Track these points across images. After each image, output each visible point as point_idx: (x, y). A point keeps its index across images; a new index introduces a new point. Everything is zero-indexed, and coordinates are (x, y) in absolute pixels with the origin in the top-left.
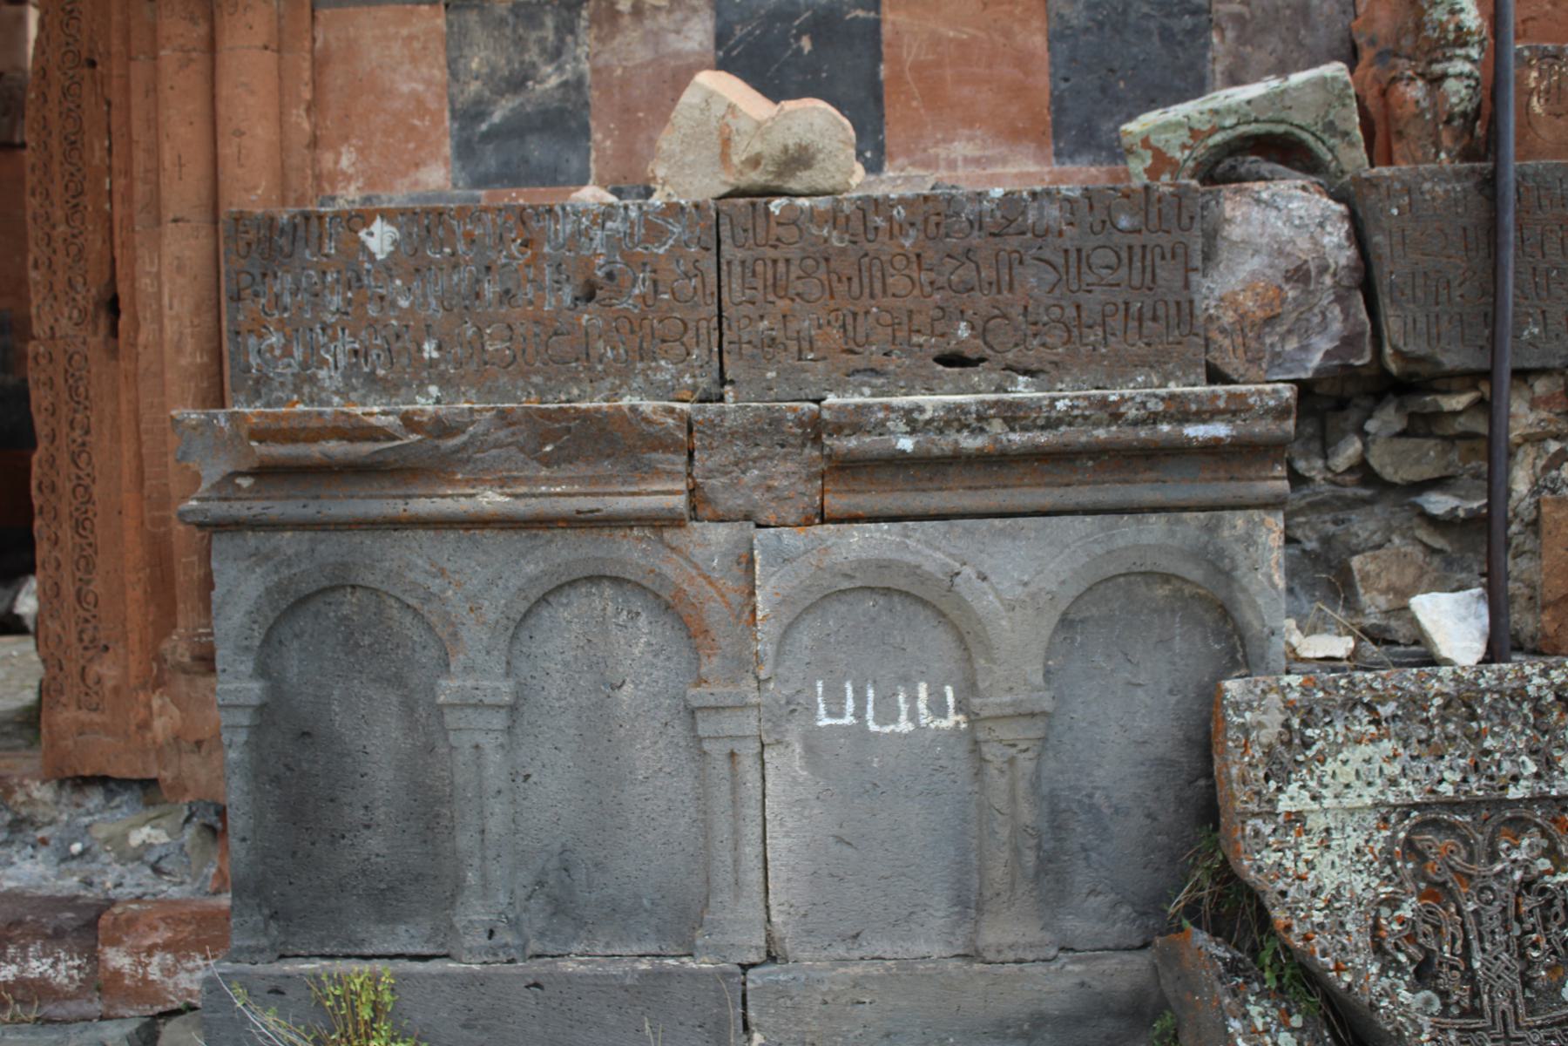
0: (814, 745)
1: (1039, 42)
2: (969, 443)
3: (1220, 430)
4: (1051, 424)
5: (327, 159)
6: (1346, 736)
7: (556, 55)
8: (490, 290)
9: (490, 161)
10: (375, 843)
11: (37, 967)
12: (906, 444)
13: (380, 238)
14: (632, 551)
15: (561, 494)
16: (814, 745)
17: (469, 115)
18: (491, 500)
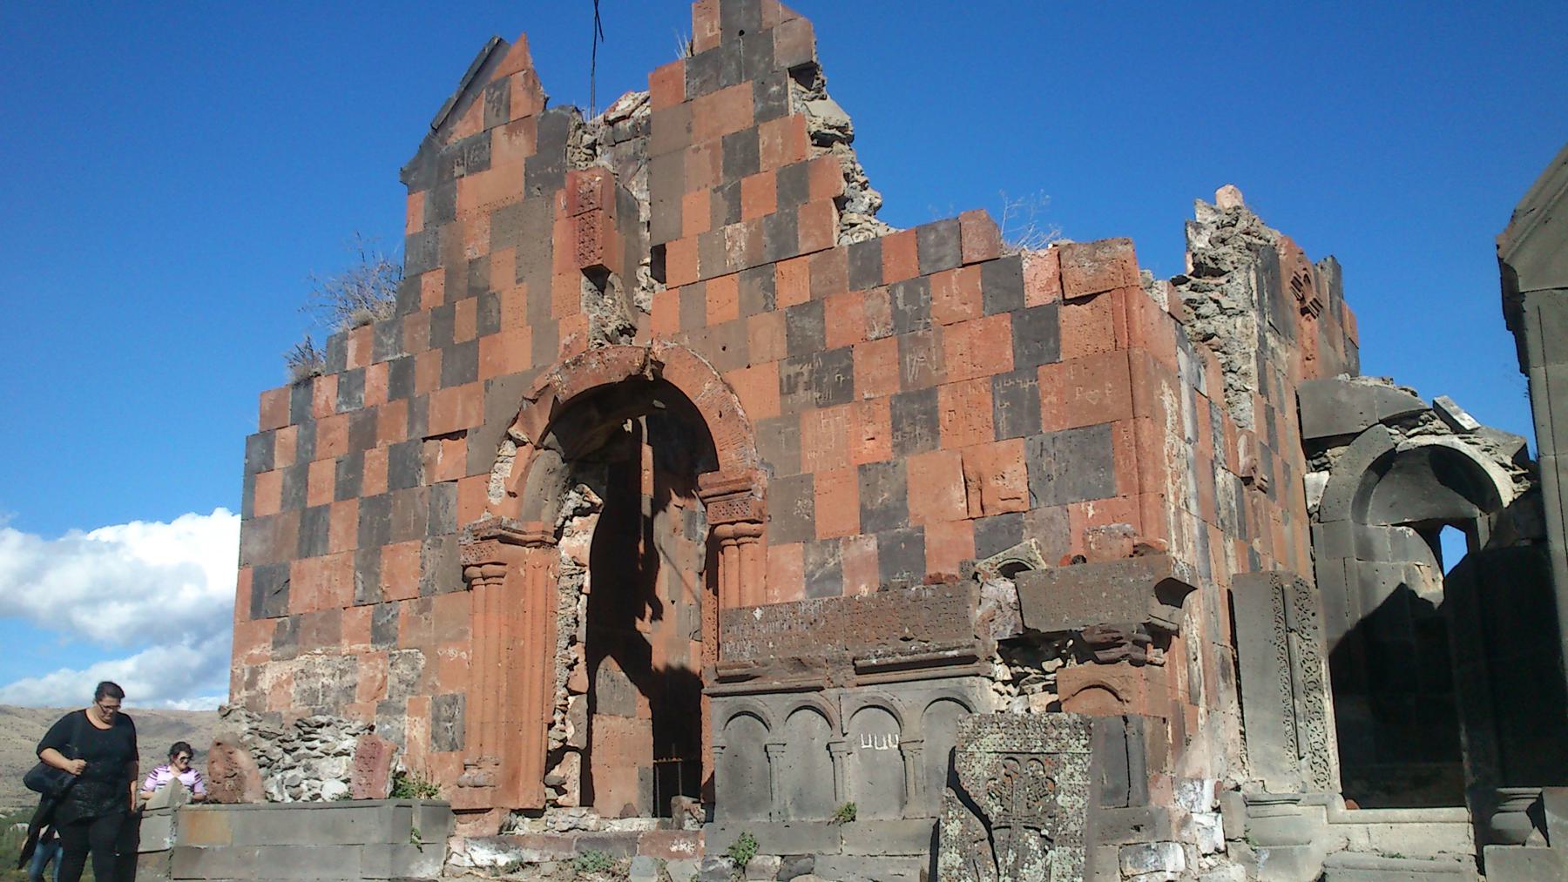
0: (862, 753)
1: (971, 538)
2: (890, 660)
3: (955, 653)
4: (912, 653)
5: (770, 592)
6: (974, 736)
8: (785, 627)
9: (815, 589)
10: (752, 789)
11: (682, 847)
12: (874, 661)
13: (758, 614)
14: (813, 696)
16: (862, 753)
17: (809, 576)
18: (776, 684)
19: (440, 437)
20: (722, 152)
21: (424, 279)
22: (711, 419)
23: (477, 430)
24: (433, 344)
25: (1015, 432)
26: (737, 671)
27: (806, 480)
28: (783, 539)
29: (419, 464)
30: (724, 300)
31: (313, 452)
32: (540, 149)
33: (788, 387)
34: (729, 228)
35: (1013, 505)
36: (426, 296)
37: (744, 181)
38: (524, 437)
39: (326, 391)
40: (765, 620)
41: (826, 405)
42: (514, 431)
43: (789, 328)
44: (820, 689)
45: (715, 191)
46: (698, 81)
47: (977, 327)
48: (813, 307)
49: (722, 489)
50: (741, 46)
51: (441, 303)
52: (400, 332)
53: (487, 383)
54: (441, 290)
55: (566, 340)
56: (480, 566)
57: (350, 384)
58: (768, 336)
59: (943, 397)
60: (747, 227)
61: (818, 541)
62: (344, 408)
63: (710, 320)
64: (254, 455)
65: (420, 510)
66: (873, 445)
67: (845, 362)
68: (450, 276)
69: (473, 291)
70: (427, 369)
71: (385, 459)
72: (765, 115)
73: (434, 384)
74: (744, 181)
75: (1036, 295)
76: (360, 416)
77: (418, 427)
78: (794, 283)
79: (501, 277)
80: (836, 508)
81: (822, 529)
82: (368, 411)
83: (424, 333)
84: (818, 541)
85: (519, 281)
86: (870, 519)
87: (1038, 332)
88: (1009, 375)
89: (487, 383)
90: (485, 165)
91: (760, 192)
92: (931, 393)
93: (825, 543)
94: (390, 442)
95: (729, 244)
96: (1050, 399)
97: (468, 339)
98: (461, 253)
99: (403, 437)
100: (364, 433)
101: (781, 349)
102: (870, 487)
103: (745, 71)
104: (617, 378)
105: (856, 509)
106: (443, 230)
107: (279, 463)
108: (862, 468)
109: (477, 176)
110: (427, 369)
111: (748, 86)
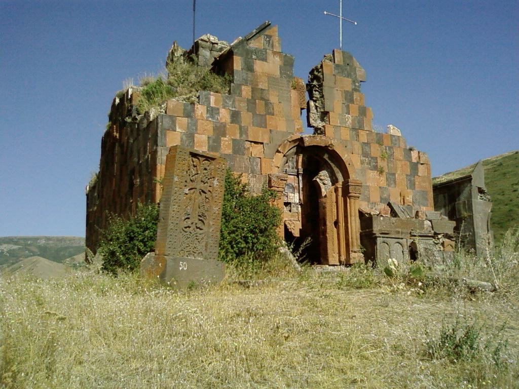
7: (375, 207)
15: (397, 236)
18: (393, 236)
19: (251, 142)
20: (344, 94)
21: (243, 87)
22: (347, 166)
23: (268, 144)
24: (248, 110)
25: (411, 188)
26: (386, 232)
27: (368, 187)
28: (362, 201)
29: (245, 148)
30: (346, 134)
31: (196, 129)
32: (284, 65)
33: (362, 163)
34: (347, 115)
35: (410, 204)
36: (244, 93)
37: (350, 105)
38: (281, 151)
39: (200, 110)
40: (383, 220)
41: (372, 170)
42: (279, 149)
43: (362, 148)
44: (402, 239)
45: (343, 104)
46: (337, 71)
47: (403, 163)
48: (367, 144)
49: (355, 184)
50: (348, 67)
51: (250, 98)
52: (234, 101)
53: (271, 131)
54: (250, 93)
55: (298, 127)
56: (278, 188)
57: (213, 112)
58: (357, 147)
59: (397, 175)
60: (352, 117)
61: (371, 202)
62: (210, 119)
63: (342, 138)
64: (164, 122)
65: (246, 164)
66: (383, 183)
67: (376, 161)
68: (253, 90)
69: (262, 99)
70: (246, 118)
71: (231, 142)
72: (355, 90)
73: (250, 124)
74: (350, 105)
75: (414, 161)
76: (218, 125)
77: (244, 136)
78: (364, 137)
79: (273, 99)
80: (375, 197)
81: (372, 200)
82: (222, 123)
83: (244, 105)
84: (371, 202)
85: (280, 102)
86: (382, 200)
87: (414, 167)
88: (410, 176)
89: (271, 131)
90: (265, 60)
91: (354, 108)
92: (394, 174)
93: (372, 203)
94: (232, 137)
95: (347, 120)
96: (417, 183)
97: (262, 113)
98: (258, 85)
99: (238, 137)
100: (220, 130)
101: (360, 152)
102: (382, 193)
103: (349, 75)
104: (323, 145)
105: (379, 197)
106: (250, 74)
107: (178, 130)
108: (380, 187)
109: (261, 62)
110: (246, 118)
111: (351, 80)
